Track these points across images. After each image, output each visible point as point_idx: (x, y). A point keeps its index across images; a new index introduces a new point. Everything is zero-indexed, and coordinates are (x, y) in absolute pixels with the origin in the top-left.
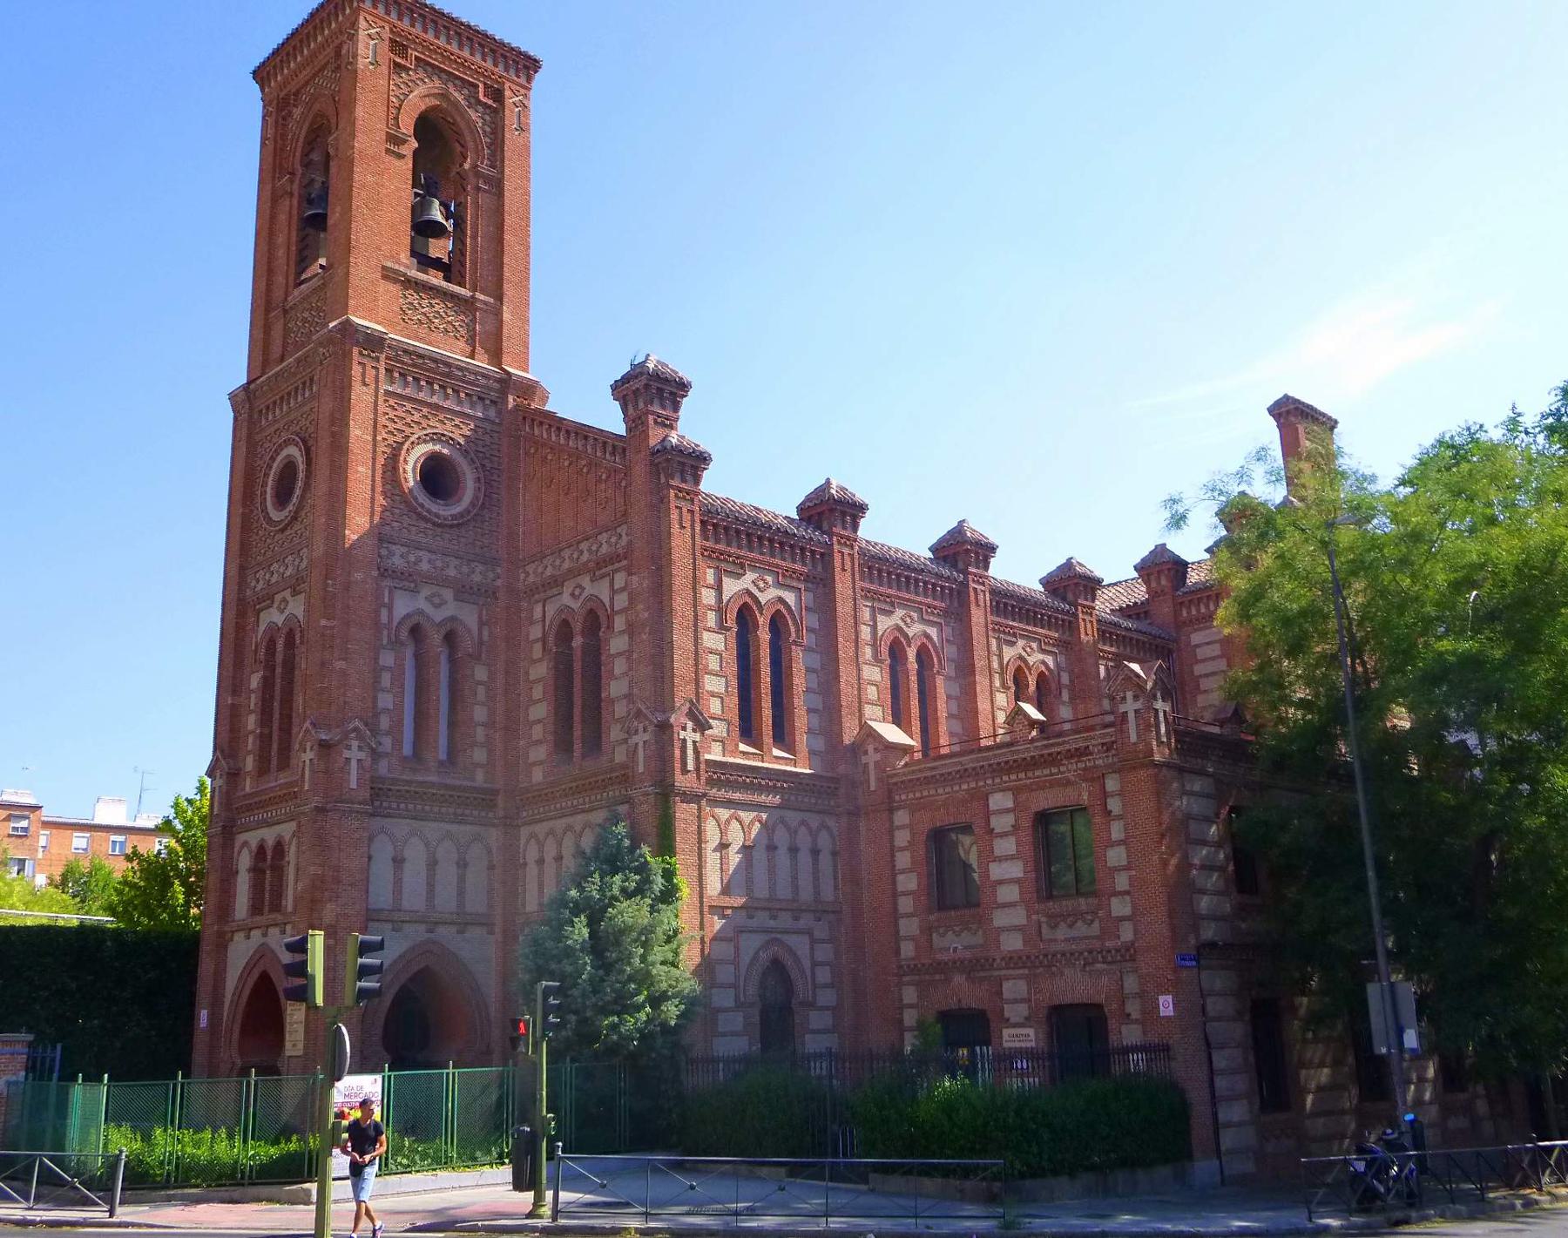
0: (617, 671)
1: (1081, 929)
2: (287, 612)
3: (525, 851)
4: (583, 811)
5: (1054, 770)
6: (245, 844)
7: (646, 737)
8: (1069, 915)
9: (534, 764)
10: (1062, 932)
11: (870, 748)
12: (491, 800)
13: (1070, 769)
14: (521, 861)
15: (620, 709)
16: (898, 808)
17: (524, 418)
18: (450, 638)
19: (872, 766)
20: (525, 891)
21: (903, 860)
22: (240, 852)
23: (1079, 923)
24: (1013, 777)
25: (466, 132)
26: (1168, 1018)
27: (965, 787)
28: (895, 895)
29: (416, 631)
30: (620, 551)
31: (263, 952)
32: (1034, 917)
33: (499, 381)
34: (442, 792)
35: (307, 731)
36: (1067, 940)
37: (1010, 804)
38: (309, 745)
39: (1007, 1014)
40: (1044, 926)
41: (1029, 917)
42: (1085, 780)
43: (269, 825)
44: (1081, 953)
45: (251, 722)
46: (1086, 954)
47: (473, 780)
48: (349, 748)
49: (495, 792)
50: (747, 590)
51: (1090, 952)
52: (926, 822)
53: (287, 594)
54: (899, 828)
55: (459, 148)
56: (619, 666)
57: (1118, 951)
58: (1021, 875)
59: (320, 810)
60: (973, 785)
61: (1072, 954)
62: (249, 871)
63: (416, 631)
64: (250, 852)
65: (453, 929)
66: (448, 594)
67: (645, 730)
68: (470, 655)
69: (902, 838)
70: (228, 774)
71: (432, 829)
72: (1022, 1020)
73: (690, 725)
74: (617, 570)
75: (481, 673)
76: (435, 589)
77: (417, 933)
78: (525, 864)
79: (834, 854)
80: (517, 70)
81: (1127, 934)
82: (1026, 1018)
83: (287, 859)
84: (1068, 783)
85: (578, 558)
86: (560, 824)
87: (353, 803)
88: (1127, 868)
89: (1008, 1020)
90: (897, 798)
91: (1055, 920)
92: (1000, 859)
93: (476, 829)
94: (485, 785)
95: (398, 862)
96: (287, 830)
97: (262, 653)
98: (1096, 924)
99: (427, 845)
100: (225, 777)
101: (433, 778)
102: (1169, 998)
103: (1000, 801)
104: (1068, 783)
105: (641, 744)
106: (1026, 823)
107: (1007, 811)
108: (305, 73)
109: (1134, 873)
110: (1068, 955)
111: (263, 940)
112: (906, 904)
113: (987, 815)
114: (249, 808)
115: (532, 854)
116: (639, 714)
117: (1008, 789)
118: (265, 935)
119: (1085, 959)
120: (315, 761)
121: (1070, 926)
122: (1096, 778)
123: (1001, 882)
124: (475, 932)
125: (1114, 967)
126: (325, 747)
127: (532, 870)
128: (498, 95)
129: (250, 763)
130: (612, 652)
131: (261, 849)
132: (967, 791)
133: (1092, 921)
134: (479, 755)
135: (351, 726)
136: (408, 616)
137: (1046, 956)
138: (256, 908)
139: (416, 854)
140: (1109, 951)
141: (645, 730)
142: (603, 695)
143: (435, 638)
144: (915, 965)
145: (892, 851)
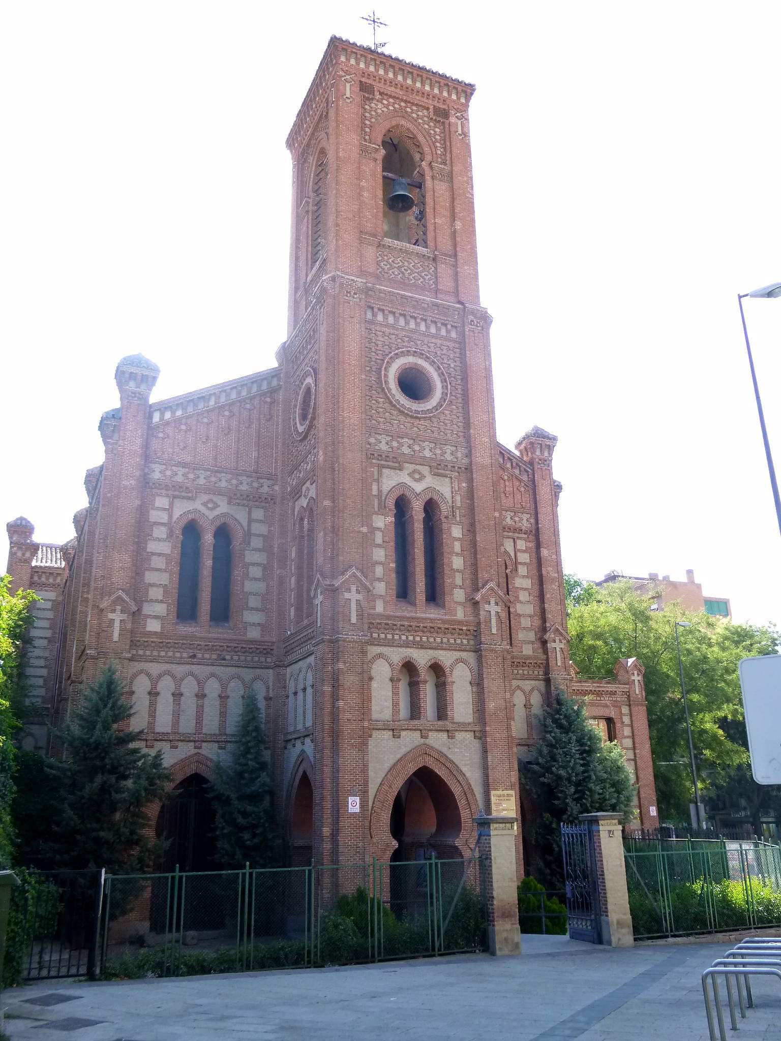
0: (522, 598)
5: (598, 699)
6: (380, 656)
13: (607, 700)
22: (372, 662)
35: (492, 589)
38: (493, 601)
42: (614, 706)
43: (421, 646)
45: (379, 554)
53: (425, 470)
74: (518, 538)
84: (606, 706)
97: (391, 503)
104: (606, 706)
122: (616, 705)
129: (380, 588)
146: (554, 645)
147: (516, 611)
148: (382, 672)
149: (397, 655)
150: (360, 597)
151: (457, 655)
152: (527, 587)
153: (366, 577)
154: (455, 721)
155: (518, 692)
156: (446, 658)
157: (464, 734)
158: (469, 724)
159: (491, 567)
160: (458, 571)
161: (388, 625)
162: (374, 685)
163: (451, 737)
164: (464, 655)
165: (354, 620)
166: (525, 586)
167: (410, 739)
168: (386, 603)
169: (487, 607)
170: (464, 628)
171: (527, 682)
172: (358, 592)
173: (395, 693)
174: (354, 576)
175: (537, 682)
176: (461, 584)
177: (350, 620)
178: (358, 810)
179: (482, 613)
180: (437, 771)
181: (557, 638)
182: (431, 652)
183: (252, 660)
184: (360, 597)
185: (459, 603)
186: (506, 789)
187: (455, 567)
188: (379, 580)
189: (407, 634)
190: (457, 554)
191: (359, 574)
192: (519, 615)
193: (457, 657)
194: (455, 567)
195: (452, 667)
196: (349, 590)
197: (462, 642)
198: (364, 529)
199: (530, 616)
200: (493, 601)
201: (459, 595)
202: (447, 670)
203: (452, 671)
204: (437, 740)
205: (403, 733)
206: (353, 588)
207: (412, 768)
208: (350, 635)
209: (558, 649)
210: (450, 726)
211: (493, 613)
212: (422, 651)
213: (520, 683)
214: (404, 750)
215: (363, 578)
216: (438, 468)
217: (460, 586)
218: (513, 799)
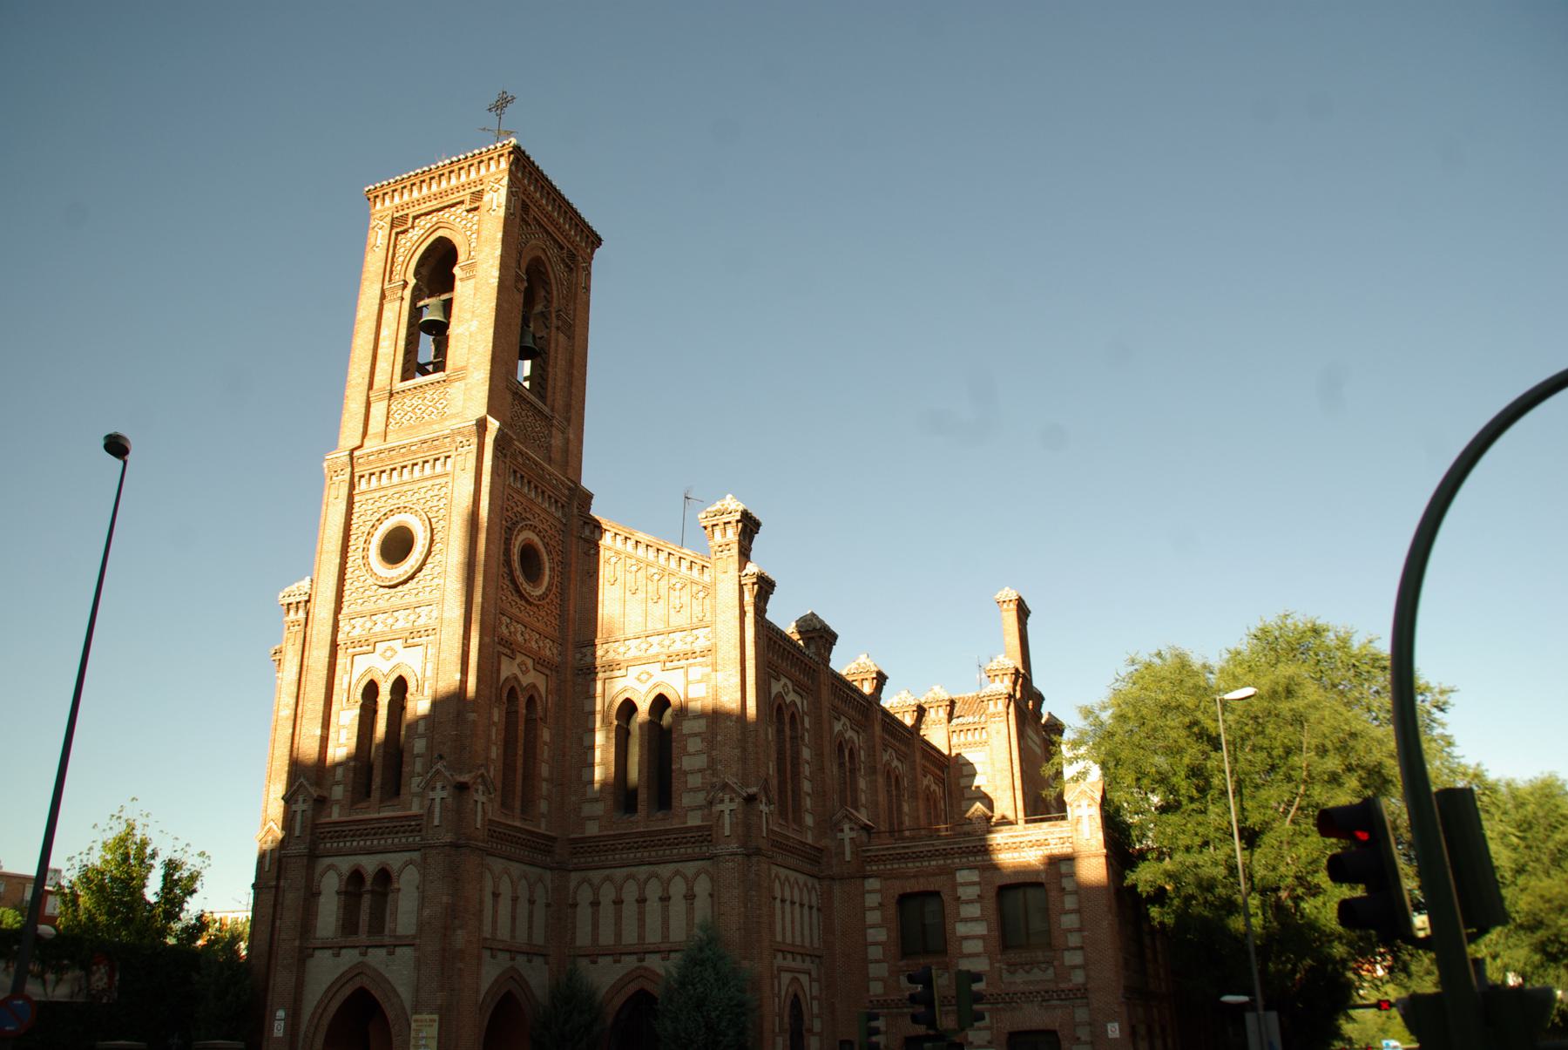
1: (1037, 974)
2: (394, 661)
3: (575, 893)
4: (650, 864)
7: (733, 806)
8: (1027, 964)
9: (589, 818)
10: (1020, 977)
11: (846, 827)
12: (551, 846)
14: (570, 901)
15: (695, 781)
16: (870, 877)
17: (585, 523)
18: (531, 701)
19: (847, 842)
20: (575, 927)
21: (873, 917)
23: (1036, 970)
24: (978, 858)
25: (553, 281)
26: (1115, 1039)
27: (933, 863)
28: (866, 945)
29: (512, 691)
30: (698, 650)
31: (359, 970)
32: (997, 965)
33: (570, 489)
34: (524, 837)
36: (1025, 983)
37: (976, 879)
38: (439, 785)
39: (970, 1039)
40: (1004, 971)
41: (991, 964)
44: (1038, 993)
46: (1043, 993)
47: (539, 828)
48: (477, 791)
49: (553, 839)
50: (781, 692)
51: (1047, 992)
52: (898, 887)
53: (398, 644)
54: (869, 892)
55: (543, 293)
56: (694, 745)
57: (1070, 990)
58: (985, 932)
59: (455, 846)
60: (942, 862)
61: (1031, 993)
62: (338, 893)
63: (512, 691)
64: (340, 875)
65: (525, 958)
66: (530, 663)
67: (731, 800)
68: (541, 719)
69: (872, 900)
70: (315, 800)
71: (516, 869)
72: (985, 1043)
73: (764, 800)
75: (546, 735)
76: (524, 658)
77: (503, 960)
78: (575, 905)
79: (819, 910)
80: (586, 243)
81: (1078, 977)
82: (990, 1042)
83: (396, 886)
85: (646, 650)
86: (619, 873)
87: (476, 840)
88: (1080, 930)
89: (971, 1043)
90: (868, 868)
91: (1013, 967)
92: (966, 920)
93: (539, 870)
94: (547, 833)
95: (496, 895)
96: (394, 861)
98: (1051, 971)
99: (512, 882)
100: (311, 802)
101: (518, 824)
102: (1116, 1025)
103: (963, 876)
105: (727, 812)
106: (992, 893)
107: (973, 884)
108: (428, 204)
109: (1086, 933)
110: (1027, 994)
111: (361, 959)
112: (875, 952)
113: (955, 886)
114: (340, 836)
115: (585, 895)
116: (725, 787)
117: (975, 868)
118: (364, 954)
119: (1042, 996)
120: (450, 800)
121: (1028, 972)
123: (966, 938)
124: (538, 961)
125: (1067, 1003)
126: (462, 788)
127: (584, 913)
128: (572, 256)
129: (338, 792)
130: (684, 732)
131: (357, 876)
132: (938, 867)
133: (1047, 969)
134: (543, 806)
135: (480, 772)
136: (507, 679)
137: (1007, 994)
138: (349, 924)
139: (505, 888)
140: (1063, 991)
141: (731, 800)
142: (674, 767)
143: (522, 701)
144: (885, 1001)
145: (864, 910)
146: (720, 807)
147: (681, 768)
148: (330, 885)
149: (345, 864)
151: (407, 856)
152: (700, 730)
155: (678, 881)
156: (394, 861)
157: (404, 949)
161: (340, 831)
162: (322, 899)
163: (391, 953)
166: (697, 730)
167: (350, 957)
170: (413, 823)
171: (691, 863)
175: (704, 862)
178: (281, 1035)
180: (373, 992)
181: (727, 797)
183: (650, 855)
186: (431, 1013)
187: (416, 751)
190: (421, 736)
192: (685, 773)
194: (416, 751)
195: (401, 871)
199: (700, 771)
201: (415, 784)
202: (394, 875)
204: (377, 957)
205: (343, 951)
206: (301, 799)
207: (347, 991)
210: (387, 940)
211: (438, 801)
213: (679, 866)
214: (340, 971)
216: (411, 638)
217: (418, 773)
218: (436, 1025)
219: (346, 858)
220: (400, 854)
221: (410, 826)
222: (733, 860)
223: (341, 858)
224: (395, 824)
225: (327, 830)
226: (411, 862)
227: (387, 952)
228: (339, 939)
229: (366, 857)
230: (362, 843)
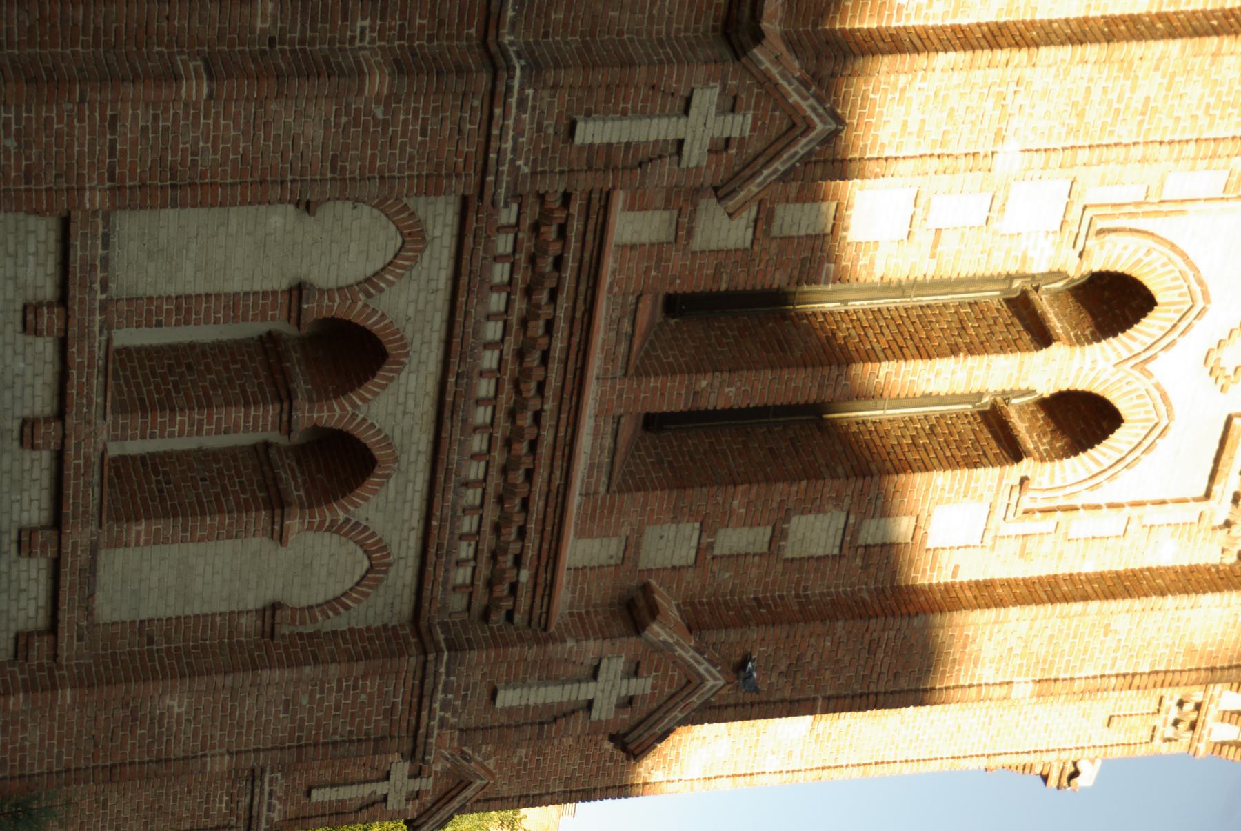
38: (641, 686)
62: (299, 290)
64: (370, 283)
150: (695, 154)
151: (405, 546)
153: (785, 177)
154: (103, 555)
157: (39, 590)
158: (89, 611)
159: (789, 674)
160: (778, 535)
162: (280, 218)
163: (25, 542)
164: (403, 574)
165: (590, 132)
168: (656, 252)
169: (614, 667)
170: (525, 575)
172: (721, 146)
173: (234, 305)
174: (793, 126)
176: (717, 552)
177: (588, 114)
179: (592, 647)
181: (426, 784)
182: (422, 441)
184: (695, 154)
185: (632, 547)
188: (762, 222)
189: (510, 346)
191: (801, 147)
193: (394, 549)
195: (354, 531)
196: (731, 105)
197: (459, 563)
198: (1009, 157)
200: (641, 686)
203: (334, 528)
208: (518, 121)
209: (381, 788)
210: (78, 536)
212: (424, 407)
215: (779, 166)
217: (711, 546)
219: (441, 300)
220: (416, 520)
221: (518, 561)
222: (231, 812)
223: (443, 278)
224: (537, 504)
225: (576, 225)
226: (376, 570)
227: (32, 531)
228: (100, 339)
229: (431, 386)
230: (489, 360)
